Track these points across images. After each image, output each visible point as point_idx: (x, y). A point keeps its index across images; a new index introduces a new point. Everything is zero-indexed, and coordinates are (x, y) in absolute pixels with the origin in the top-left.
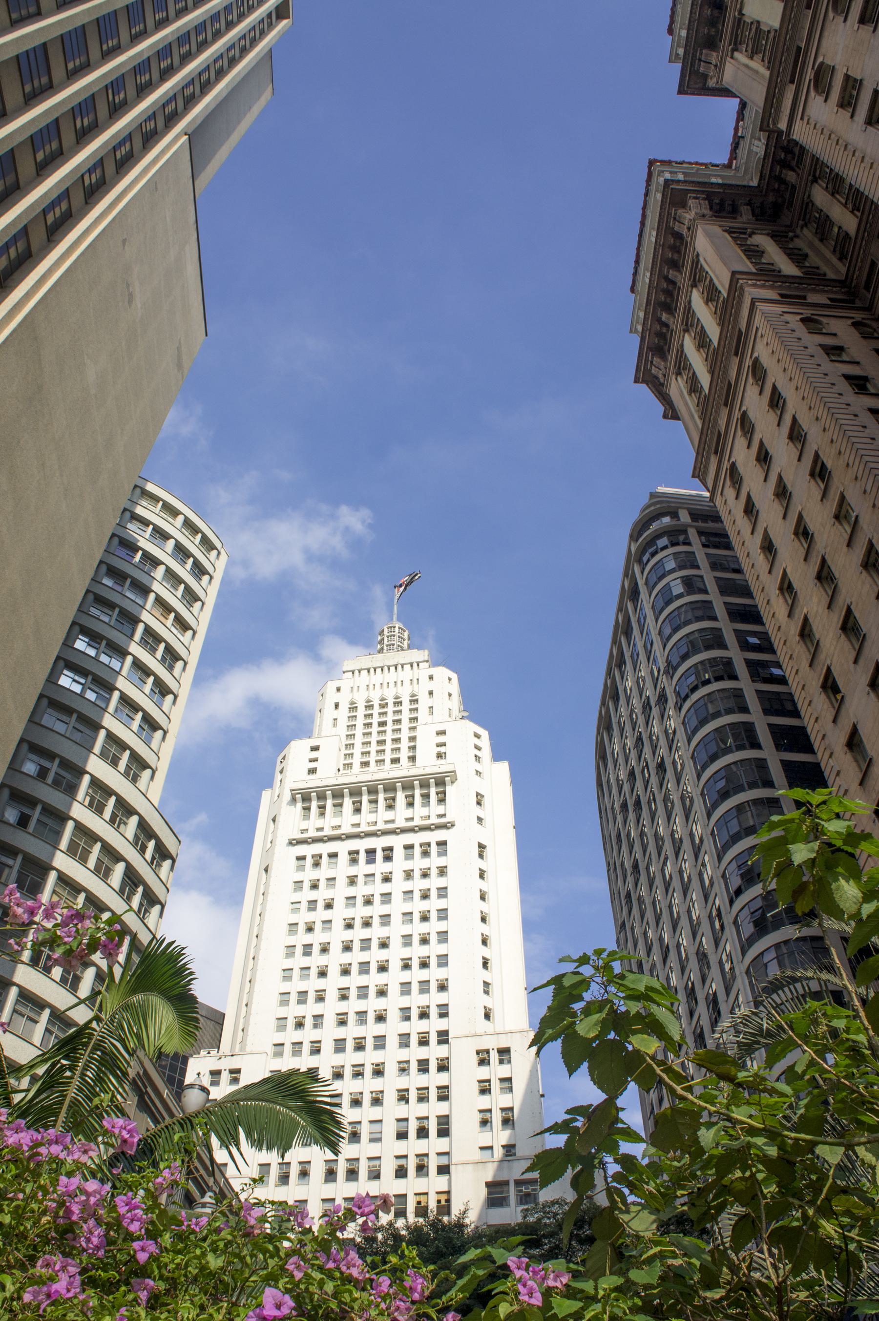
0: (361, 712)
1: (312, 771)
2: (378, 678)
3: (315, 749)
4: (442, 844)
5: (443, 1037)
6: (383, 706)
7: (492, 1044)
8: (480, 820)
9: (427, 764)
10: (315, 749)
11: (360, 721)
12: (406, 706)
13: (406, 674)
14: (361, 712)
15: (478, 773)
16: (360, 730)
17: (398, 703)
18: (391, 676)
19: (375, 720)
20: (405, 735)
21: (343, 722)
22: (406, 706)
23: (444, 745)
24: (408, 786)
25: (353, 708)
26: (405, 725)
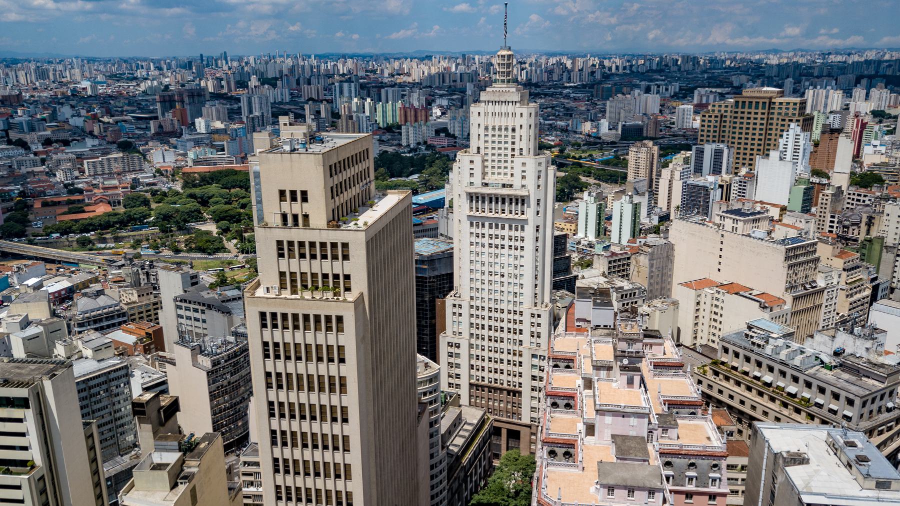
0: (490, 132)
1: (472, 175)
2: (498, 108)
3: (472, 162)
10: (472, 162)
12: (510, 133)
13: (510, 108)
14: (490, 132)
15: (539, 186)
17: (506, 129)
18: (504, 108)
23: (524, 171)
25: (486, 128)
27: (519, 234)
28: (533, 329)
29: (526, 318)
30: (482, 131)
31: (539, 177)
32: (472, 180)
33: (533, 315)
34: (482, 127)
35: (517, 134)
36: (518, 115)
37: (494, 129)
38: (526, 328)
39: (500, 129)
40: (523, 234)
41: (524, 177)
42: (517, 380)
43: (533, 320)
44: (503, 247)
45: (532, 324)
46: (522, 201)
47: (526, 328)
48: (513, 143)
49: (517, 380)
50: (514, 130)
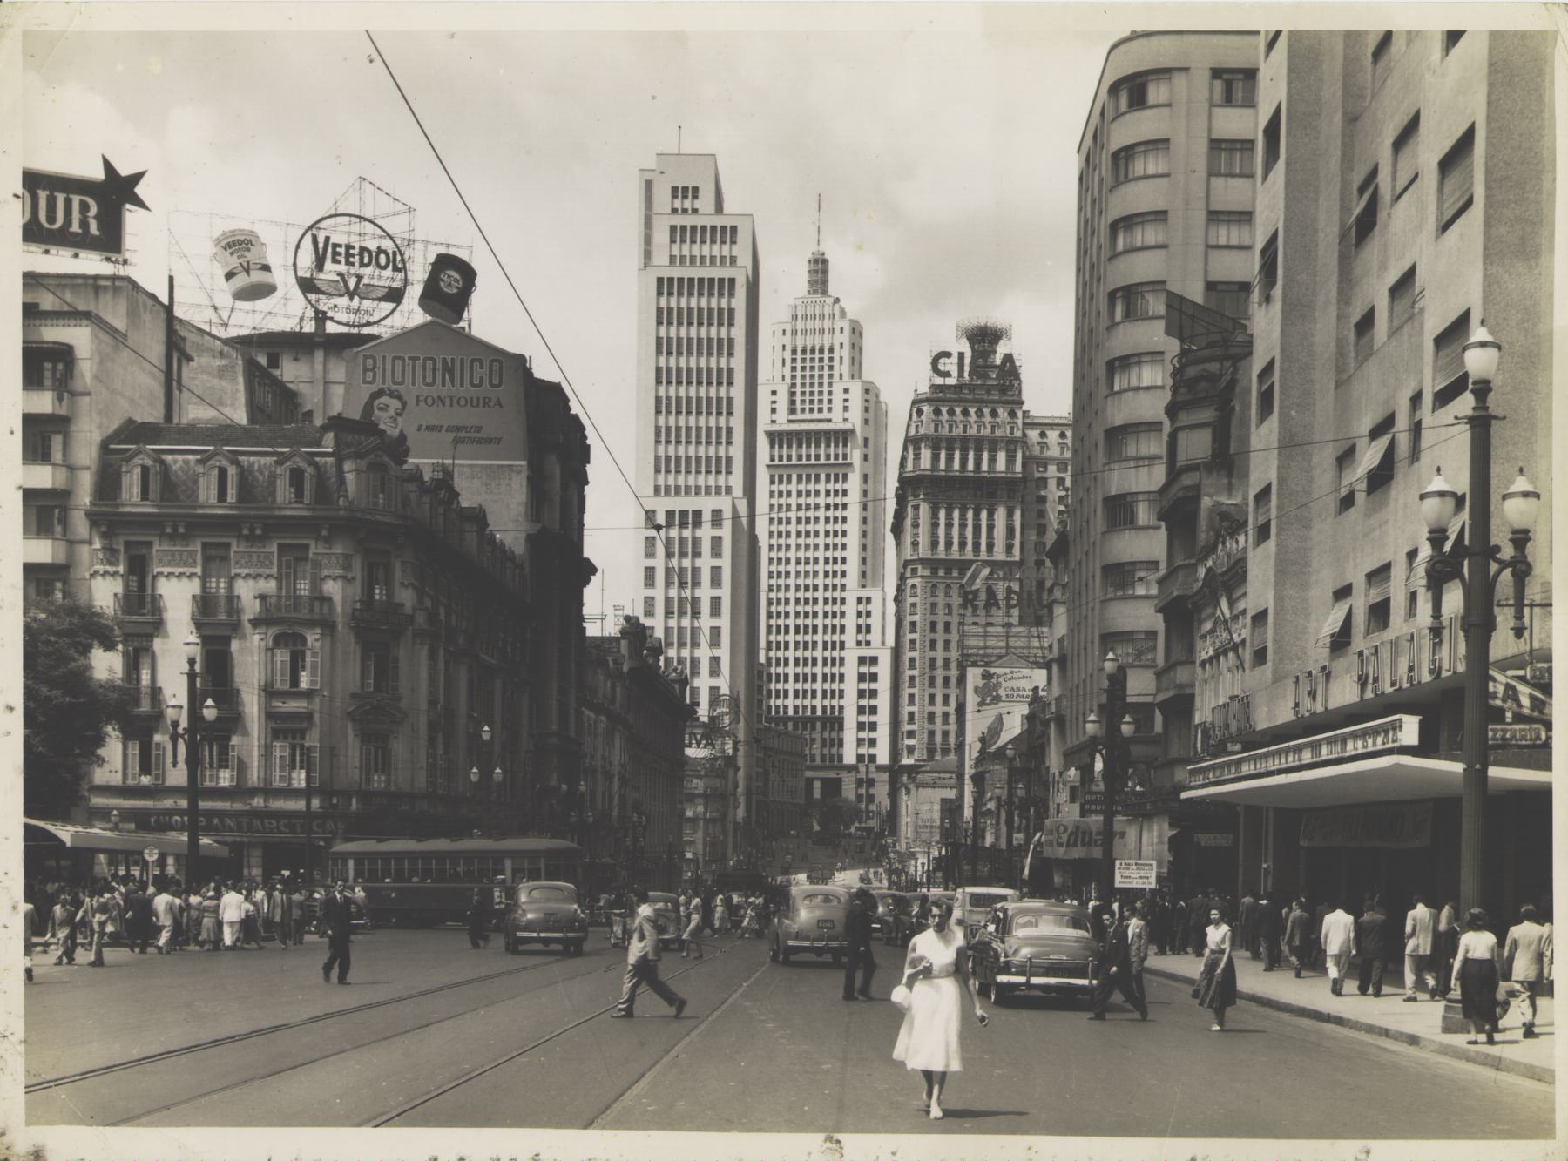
0: (799, 356)
1: (773, 411)
4: (845, 477)
5: (843, 587)
6: (813, 351)
7: (864, 594)
8: (866, 458)
9: (837, 423)
10: (774, 393)
11: (799, 365)
12: (826, 356)
14: (799, 356)
15: (866, 422)
16: (799, 373)
17: (822, 351)
19: (808, 364)
20: (826, 380)
21: (788, 362)
22: (826, 356)
24: (827, 433)
25: (794, 352)
26: (826, 372)
27: (839, 486)
28: (861, 621)
29: (851, 608)
30: (788, 355)
31: (867, 410)
32: (774, 417)
33: (860, 600)
34: (789, 348)
35: (836, 356)
36: (837, 331)
37: (804, 352)
38: (851, 622)
39: (813, 351)
40: (846, 486)
41: (846, 409)
42: (835, 702)
43: (861, 608)
44: (817, 507)
45: (859, 614)
46: (843, 436)
47: (851, 622)
48: (831, 368)
49: (835, 702)
50: (831, 350)
